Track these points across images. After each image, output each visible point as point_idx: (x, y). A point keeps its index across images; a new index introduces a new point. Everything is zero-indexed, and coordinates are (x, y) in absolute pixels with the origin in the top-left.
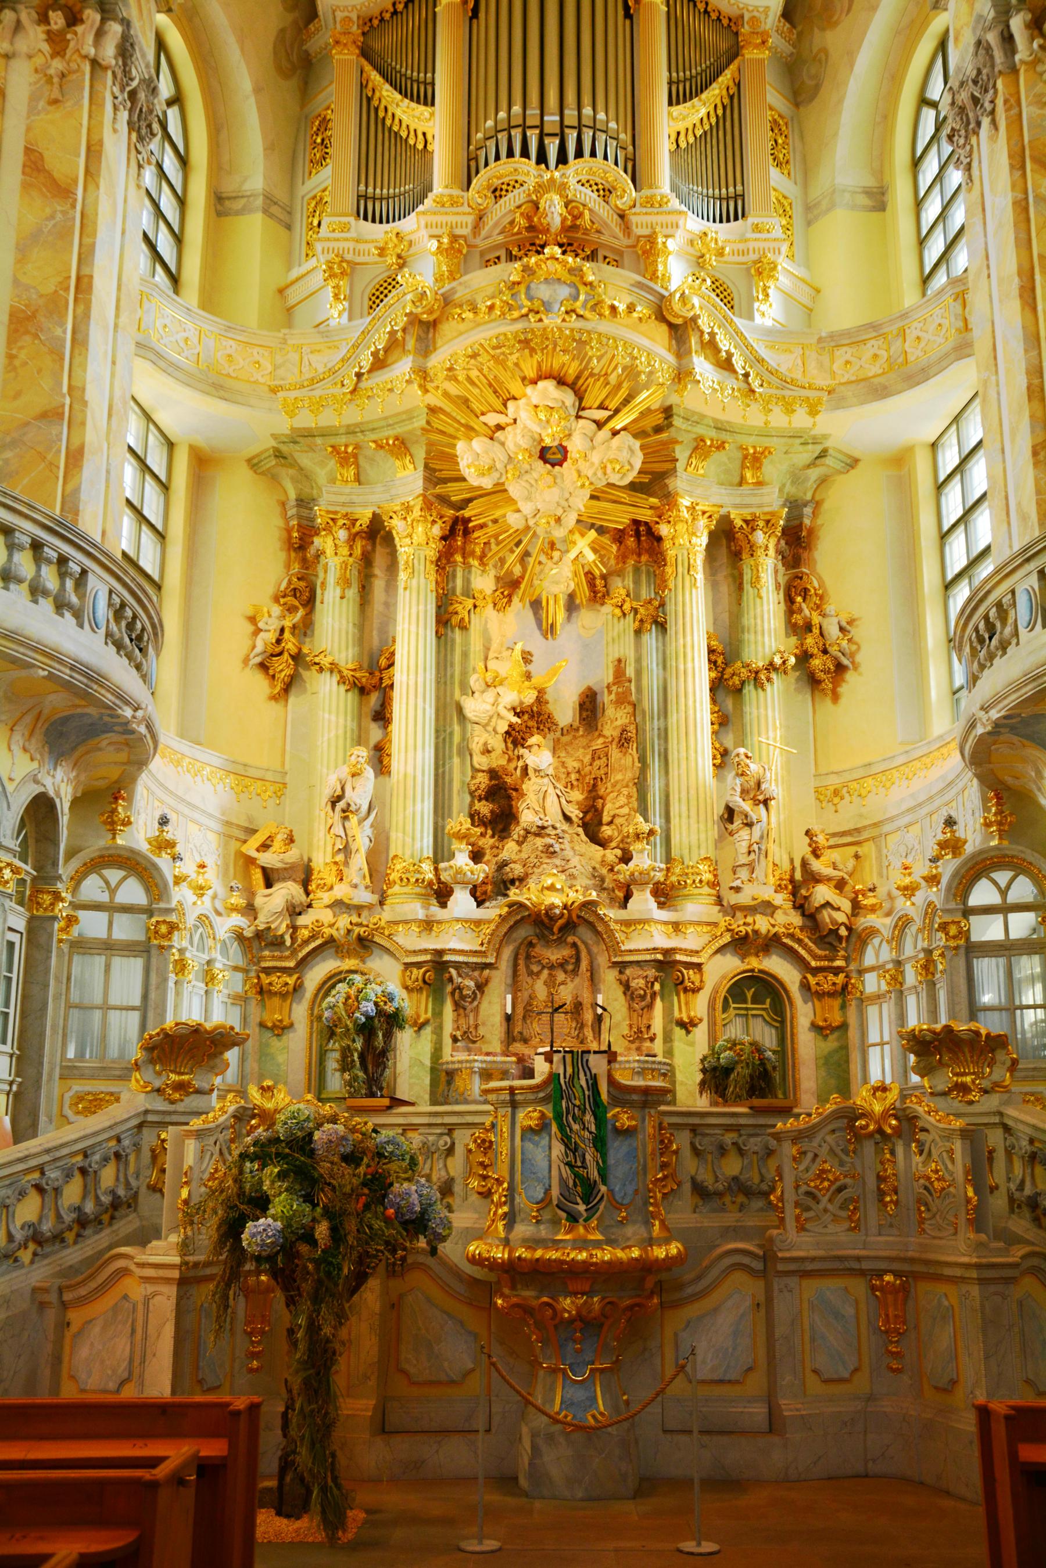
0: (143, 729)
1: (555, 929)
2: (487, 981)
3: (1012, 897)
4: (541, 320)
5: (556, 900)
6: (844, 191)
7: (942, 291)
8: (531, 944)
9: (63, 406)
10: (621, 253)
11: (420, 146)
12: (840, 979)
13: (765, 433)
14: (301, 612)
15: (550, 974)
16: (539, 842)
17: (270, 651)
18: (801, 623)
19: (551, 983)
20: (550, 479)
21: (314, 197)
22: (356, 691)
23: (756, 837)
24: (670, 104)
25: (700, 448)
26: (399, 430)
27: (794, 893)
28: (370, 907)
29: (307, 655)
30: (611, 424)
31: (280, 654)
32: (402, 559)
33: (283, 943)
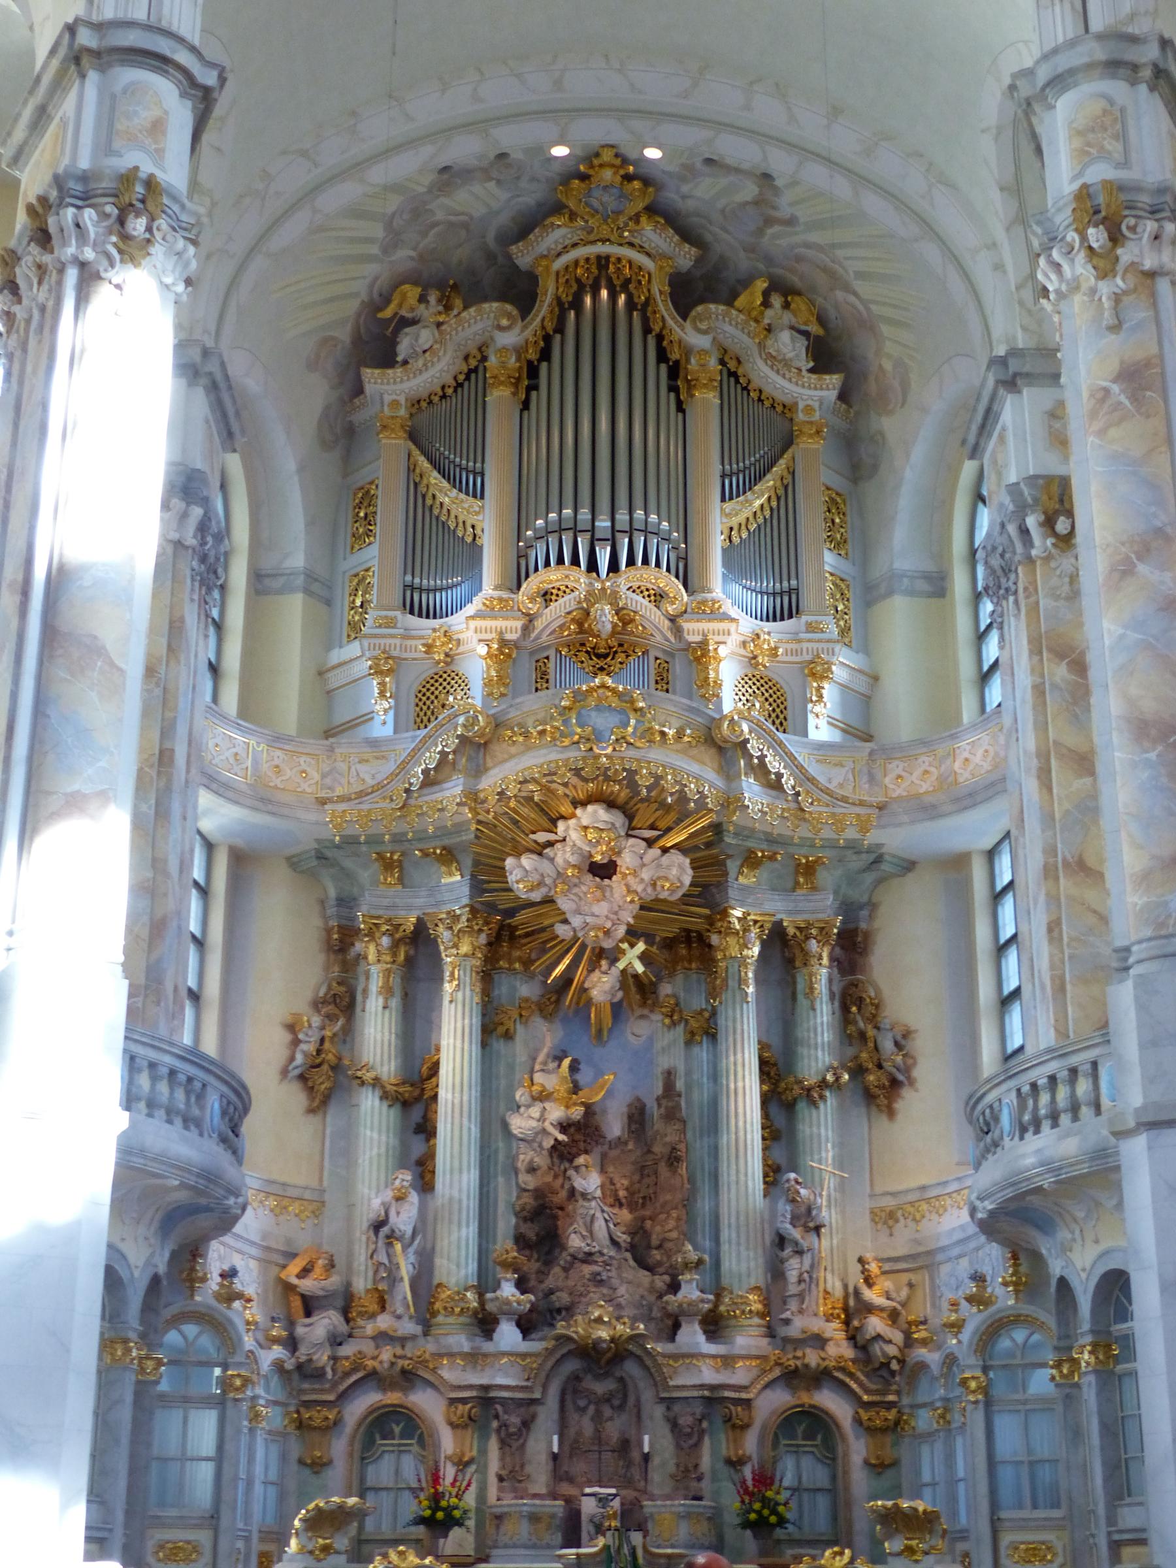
1: (603, 1362)
6: (903, 576)
11: (469, 540)
12: (892, 1415)
16: (587, 1270)
17: (310, 1062)
19: (598, 1418)
20: (599, 893)
21: (356, 575)
22: (398, 1106)
23: (806, 1266)
24: (723, 500)
25: (751, 861)
26: (446, 842)
27: (847, 1323)
29: (349, 1068)
30: (661, 843)
31: (319, 1066)
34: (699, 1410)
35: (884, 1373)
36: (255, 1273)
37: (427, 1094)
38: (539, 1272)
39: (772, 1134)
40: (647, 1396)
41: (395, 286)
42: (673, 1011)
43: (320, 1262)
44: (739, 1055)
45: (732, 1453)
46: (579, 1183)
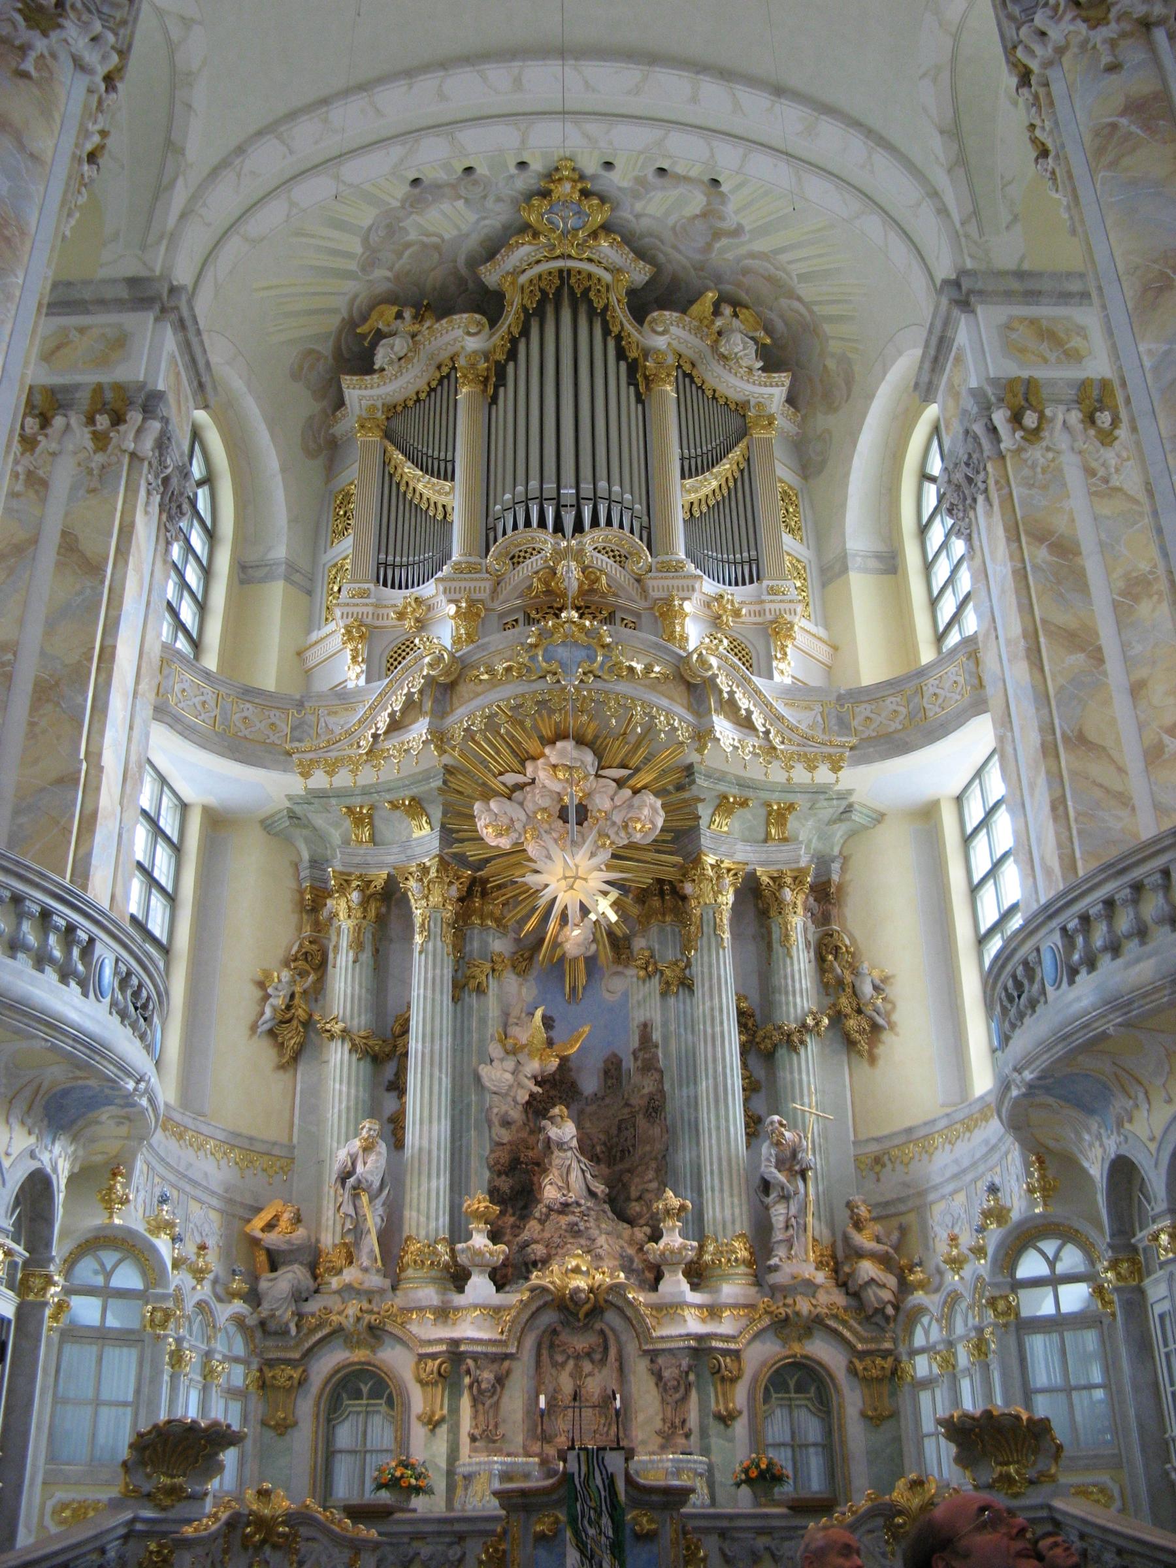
0: (144, 1102)
1: (581, 1315)
2: (508, 1372)
3: (1060, 1268)
4: (558, 681)
5: (581, 1283)
6: (855, 555)
7: (954, 650)
8: (555, 1332)
9: (79, 771)
10: (638, 615)
11: (439, 517)
12: (888, 1363)
13: (789, 788)
14: (312, 978)
15: (576, 1365)
16: (564, 1220)
18: (833, 982)
19: (577, 1374)
21: (335, 565)
22: (369, 1059)
24: (683, 477)
25: (723, 805)
26: (415, 791)
27: (836, 1271)
28: (381, 1292)
30: (631, 782)
31: (289, 1021)
32: (418, 921)
33: (286, 1332)
34: (685, 1363)
35: (878, 1319)
36: (216, 1226)
37: (400, 1051)
38: (513, 1226)
39: (751, 1088)
40: (631, 1348)
41: (372, 308)
42: (647, 963)
43: (286, 1216)
44: (716, 1000)
45: (722, 1408)
46: (553, 1132)
